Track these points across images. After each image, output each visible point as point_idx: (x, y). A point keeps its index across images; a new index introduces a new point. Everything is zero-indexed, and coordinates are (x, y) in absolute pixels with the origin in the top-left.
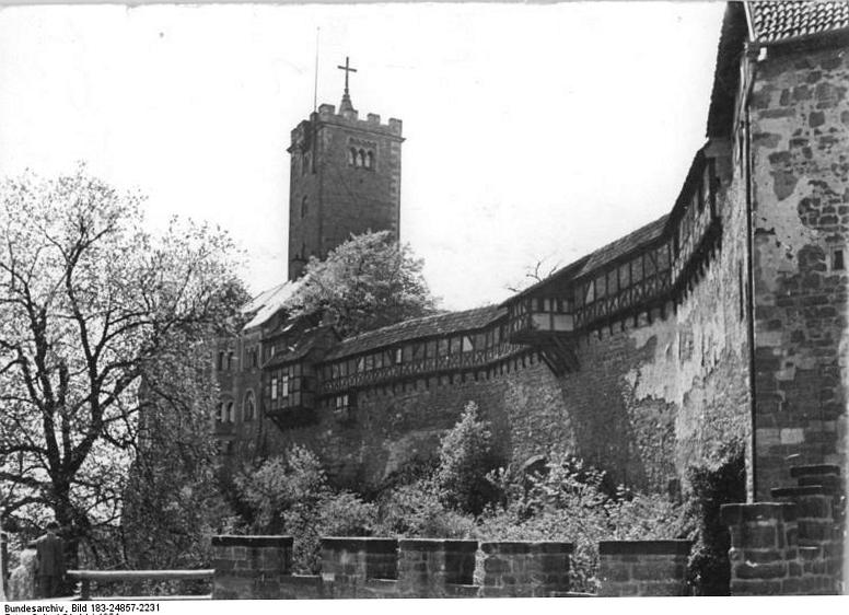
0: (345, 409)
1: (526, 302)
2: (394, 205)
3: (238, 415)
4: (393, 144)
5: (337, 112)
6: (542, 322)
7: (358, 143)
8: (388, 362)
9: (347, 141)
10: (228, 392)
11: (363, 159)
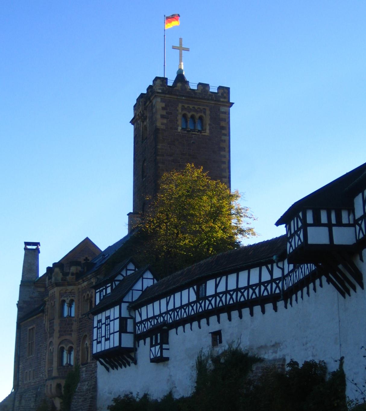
0: (158, 347)
1: (301, 214)
2: (224, 163)
3: (76, 359)
4: (223, 109)
5: (170, 84)
6: (318, 236)
7: (189, 110)
8: (193, 298)
9: (179, 108)
10: (68, 337)
11: (194, 123)
